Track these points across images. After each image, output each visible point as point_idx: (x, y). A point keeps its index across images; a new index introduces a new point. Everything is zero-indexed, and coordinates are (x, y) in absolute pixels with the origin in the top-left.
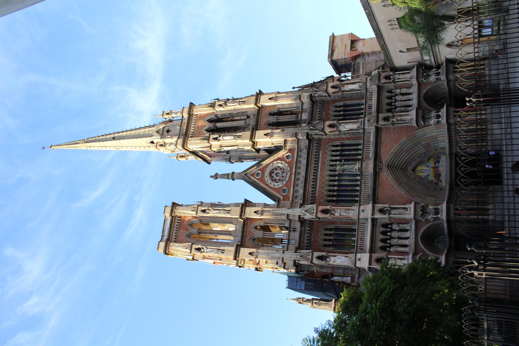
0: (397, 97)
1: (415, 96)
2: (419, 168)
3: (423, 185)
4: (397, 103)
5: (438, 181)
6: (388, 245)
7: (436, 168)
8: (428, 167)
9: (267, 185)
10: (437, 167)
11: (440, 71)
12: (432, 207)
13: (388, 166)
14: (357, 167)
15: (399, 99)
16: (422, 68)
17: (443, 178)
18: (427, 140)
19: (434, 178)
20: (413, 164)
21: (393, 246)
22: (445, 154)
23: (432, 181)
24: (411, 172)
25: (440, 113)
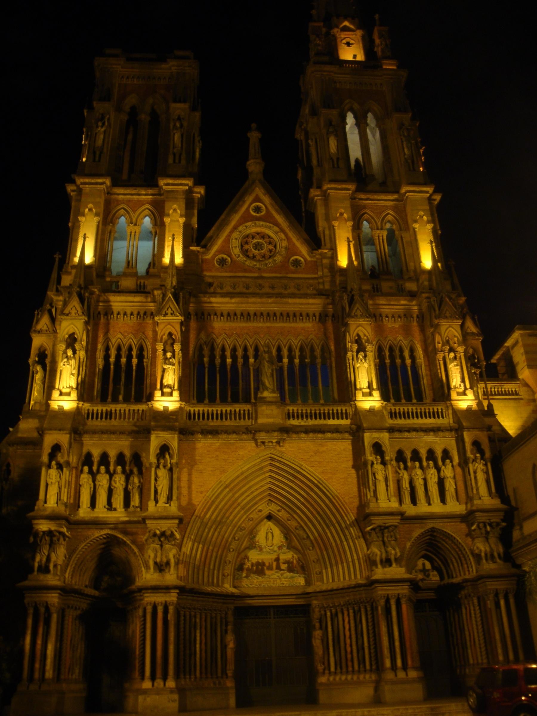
0: (433, 471)
1: (437, 508)
3: (234, 538)
4: (419, 472)
5: (248, 570)
6: (95, 468)
9: (235, 228)
11: (498, 560)
12: (171, 556)
13: (272, 459)
14: (266, 394)
15: (428, 477)
16: (503, 521)
18: (335, 541)
19: (254, 561)
20: (282, 515)
21: (94, 481)
22: (308, 582)
24: (265, 513)
25: (394, 565)
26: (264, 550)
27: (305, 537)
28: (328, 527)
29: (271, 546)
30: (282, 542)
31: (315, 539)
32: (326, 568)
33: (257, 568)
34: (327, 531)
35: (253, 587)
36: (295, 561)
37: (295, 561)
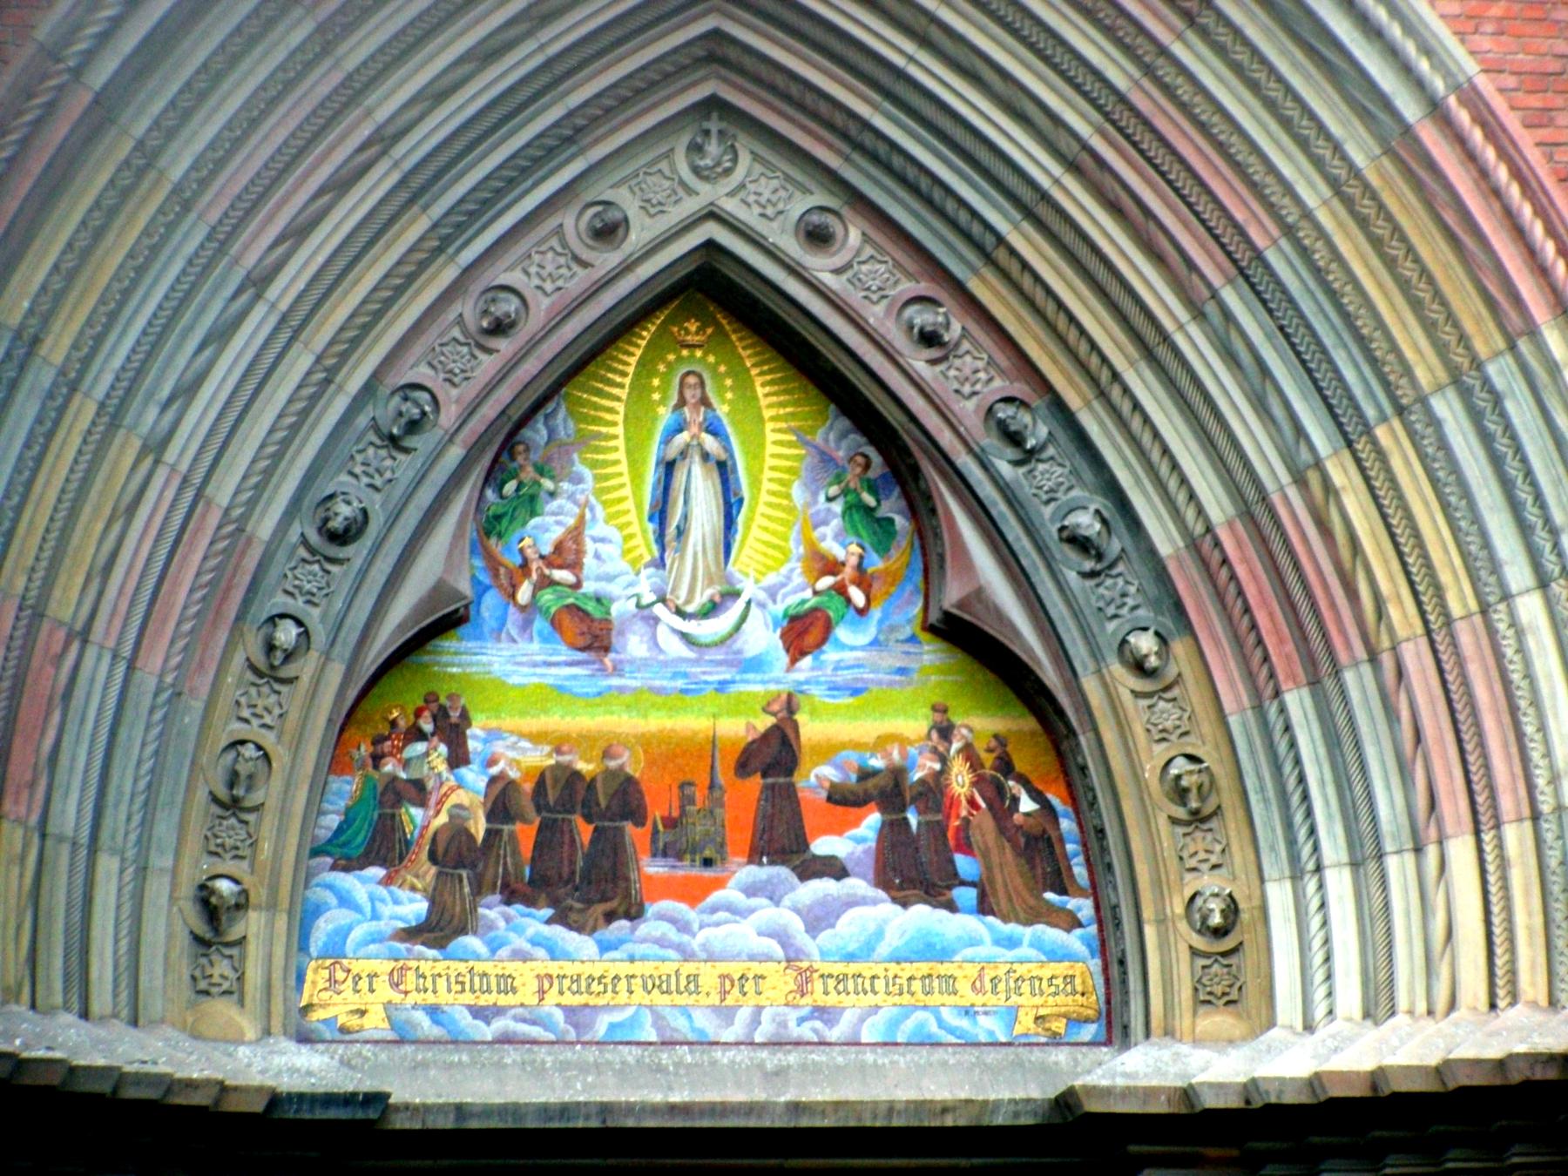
2: (774, 437)
3: (311, 498)
5: (454, 853)
7: (767, 799)
8: (804, 632)
10: (783, 842)
17: (526, 960)
19: (524, 759)
20: (856, 286)
23: (453, 731)
26: (634, 645)
27: (1085, 521)
28: (1351, 431)
29: (712, 609)
31: (1203, 546)
32: (1304, 868)
33: (551, 835)
34: (1342, 473)
35: (506, 1039)
36: (960, 780)
37: (960, 780)
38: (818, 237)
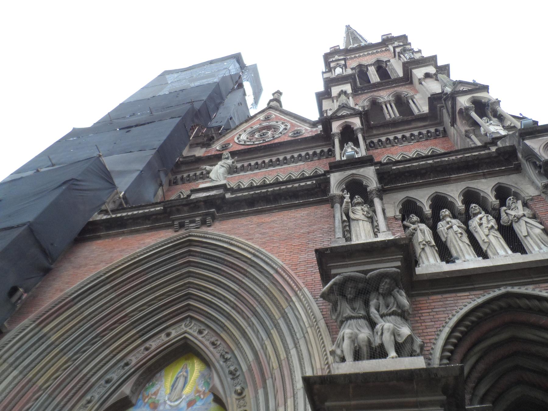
4: (456, 223)
13: (190, 243)
26: (161, 408)
30: (198, 391)
38: (200, 332)
